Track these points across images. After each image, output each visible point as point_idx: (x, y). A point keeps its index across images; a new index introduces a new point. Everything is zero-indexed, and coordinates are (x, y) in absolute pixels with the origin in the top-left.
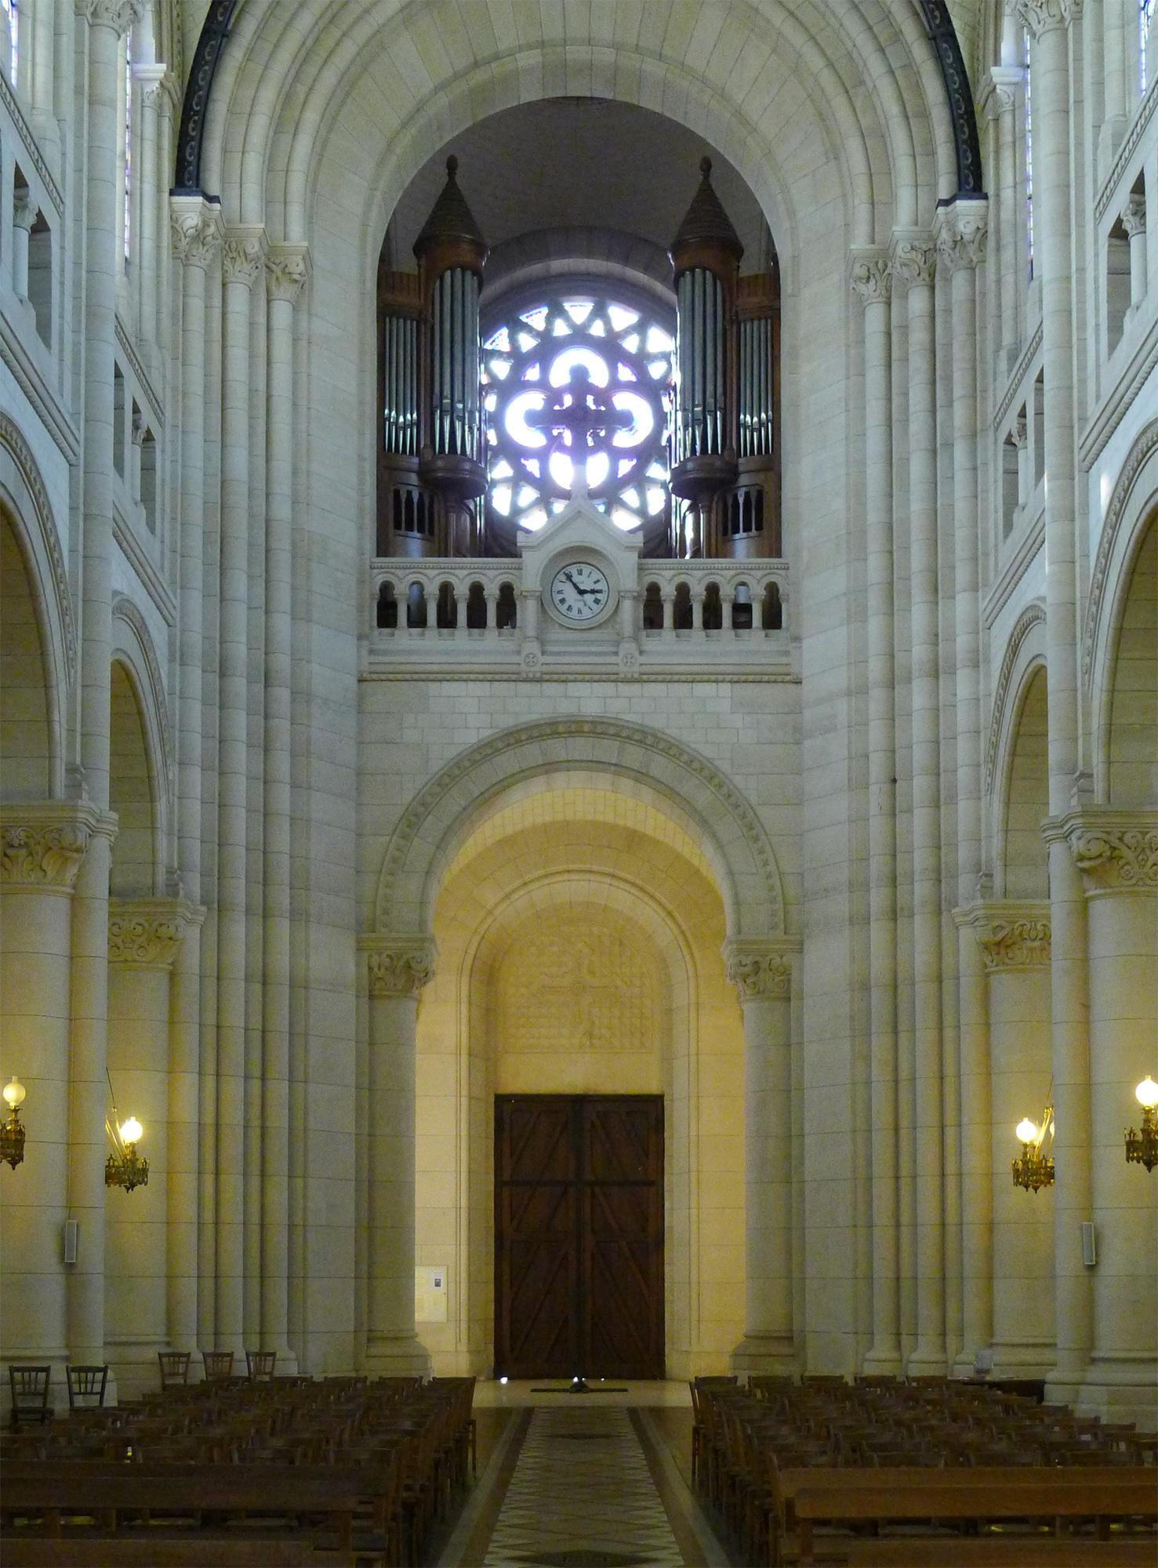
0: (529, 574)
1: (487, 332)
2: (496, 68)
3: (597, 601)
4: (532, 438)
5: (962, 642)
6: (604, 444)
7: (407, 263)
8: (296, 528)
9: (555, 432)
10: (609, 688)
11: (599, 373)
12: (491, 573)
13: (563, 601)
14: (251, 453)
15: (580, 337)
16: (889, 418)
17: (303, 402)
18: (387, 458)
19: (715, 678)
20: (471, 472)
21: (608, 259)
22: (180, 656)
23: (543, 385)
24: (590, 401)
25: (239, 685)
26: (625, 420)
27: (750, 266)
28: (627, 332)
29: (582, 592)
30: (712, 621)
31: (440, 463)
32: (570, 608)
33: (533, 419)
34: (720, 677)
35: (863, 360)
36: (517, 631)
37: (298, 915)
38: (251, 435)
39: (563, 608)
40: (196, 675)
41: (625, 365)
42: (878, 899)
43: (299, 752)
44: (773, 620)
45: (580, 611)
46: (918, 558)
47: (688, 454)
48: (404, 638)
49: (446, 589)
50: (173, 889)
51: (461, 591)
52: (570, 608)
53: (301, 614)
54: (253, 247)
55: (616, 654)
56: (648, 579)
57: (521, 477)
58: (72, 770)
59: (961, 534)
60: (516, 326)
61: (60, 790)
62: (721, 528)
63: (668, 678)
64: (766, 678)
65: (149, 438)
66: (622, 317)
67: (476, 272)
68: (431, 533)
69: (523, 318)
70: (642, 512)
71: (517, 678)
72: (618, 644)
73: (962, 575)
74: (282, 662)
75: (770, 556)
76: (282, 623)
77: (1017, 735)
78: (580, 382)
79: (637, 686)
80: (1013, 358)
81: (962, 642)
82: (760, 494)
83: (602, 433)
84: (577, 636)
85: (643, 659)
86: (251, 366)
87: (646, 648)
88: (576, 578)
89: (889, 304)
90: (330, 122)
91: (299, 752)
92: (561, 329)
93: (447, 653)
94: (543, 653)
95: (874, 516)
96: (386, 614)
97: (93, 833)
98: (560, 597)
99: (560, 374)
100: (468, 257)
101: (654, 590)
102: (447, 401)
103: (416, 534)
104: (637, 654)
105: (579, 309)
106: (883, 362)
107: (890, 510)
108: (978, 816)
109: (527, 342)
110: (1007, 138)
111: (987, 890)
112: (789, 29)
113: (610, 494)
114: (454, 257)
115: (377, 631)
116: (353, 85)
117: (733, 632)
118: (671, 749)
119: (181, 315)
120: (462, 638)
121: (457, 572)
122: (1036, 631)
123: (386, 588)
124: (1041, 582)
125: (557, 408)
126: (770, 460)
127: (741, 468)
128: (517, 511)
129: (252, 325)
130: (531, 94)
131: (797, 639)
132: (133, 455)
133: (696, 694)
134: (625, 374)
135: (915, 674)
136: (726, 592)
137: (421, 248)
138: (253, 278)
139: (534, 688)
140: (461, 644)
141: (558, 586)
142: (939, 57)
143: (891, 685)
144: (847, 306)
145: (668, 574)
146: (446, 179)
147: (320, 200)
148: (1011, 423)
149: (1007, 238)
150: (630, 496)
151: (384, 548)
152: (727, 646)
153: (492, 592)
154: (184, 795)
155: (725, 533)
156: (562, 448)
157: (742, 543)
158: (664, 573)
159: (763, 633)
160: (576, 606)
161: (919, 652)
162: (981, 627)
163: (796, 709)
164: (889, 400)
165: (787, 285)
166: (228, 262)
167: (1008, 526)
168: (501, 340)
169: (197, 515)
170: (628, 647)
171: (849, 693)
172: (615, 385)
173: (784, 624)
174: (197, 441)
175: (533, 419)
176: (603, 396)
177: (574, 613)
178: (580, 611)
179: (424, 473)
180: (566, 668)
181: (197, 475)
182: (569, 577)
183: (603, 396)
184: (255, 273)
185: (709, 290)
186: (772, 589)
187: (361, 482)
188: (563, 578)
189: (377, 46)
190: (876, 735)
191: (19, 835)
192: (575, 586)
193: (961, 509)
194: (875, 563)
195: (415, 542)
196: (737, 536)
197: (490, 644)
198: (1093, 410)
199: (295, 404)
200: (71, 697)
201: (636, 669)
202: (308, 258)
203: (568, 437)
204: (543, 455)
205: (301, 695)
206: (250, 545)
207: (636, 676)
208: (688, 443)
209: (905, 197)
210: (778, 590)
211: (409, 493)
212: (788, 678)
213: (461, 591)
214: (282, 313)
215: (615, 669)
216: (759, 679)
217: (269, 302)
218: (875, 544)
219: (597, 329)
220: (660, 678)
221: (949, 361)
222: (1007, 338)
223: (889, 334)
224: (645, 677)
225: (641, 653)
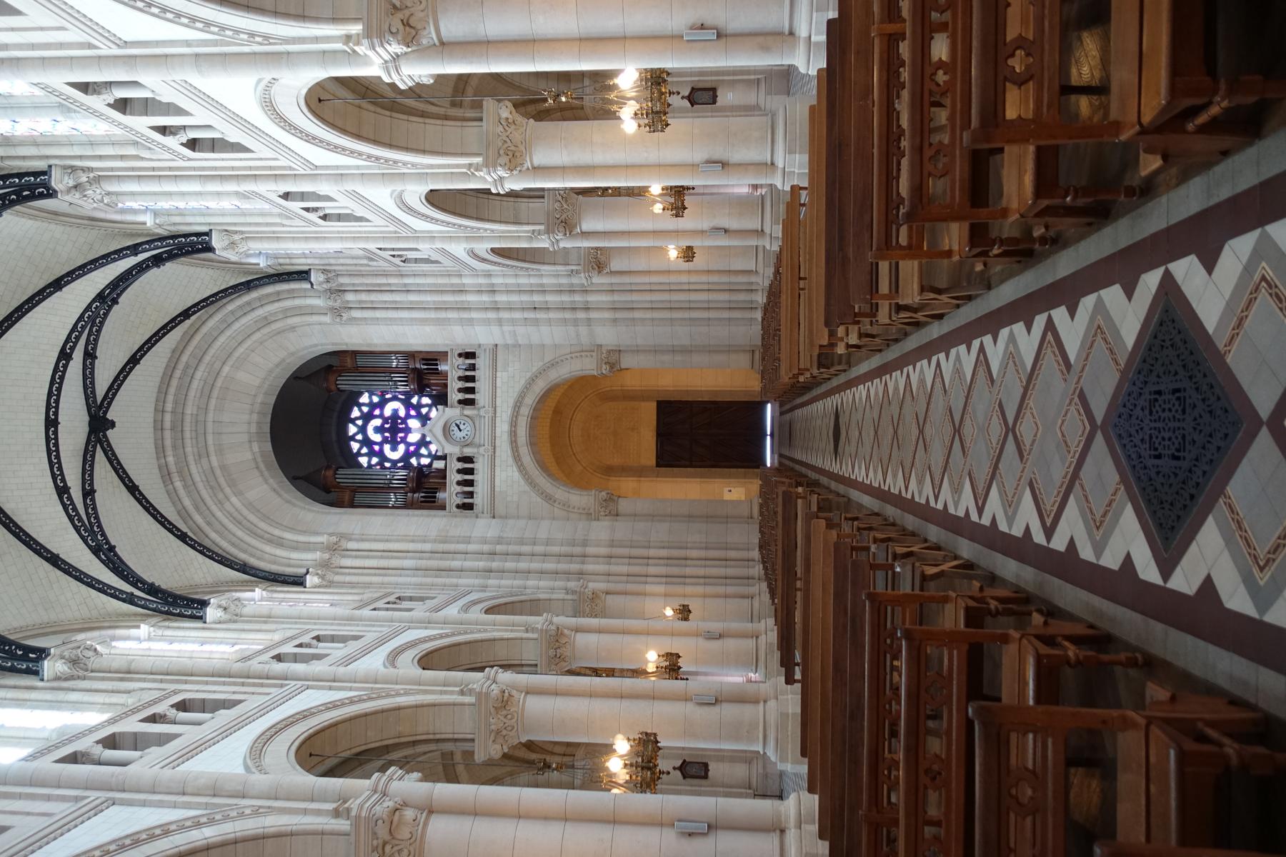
0: (453, 450)
4: (402, 448)
5: (482, 281)
6: (404, 421)
7: (333, 496)
8: (435, 541)
15: (363, 430)
18: (408, 505)
22: (484, 588)
23: (381, 444)
25: (495, 565)
27: (334, 362)
28: (361, 410)
30: (472, 379)
33: (394, 449)
37: (585, 543)
40: (491, 582)
42: (581, 315)
43: (521, 542)
44: (471, 355)
46: (449, 298)
48: (478, 500)
49: (459, 483)
50: (574, 592)
51: (460, 477)
53: (468, 540)
54: (327, 556)
58: (527, 631)
59: (440, 281)
61: (535, 636)
65: (399, 598)
70: (430, 406)
73: (455, 281)
74: (486, 548)
76: (471, 547)
77: (518, 260)
80: (372, 260)
81: (482, 281)
90: (278, 525)
91: (521, 542)
92: (359, 437)
95: (432, 315)
96: (469, 507)
97: (551, 623)
99: (377, 438)
101: (460, 402)
108: (549, 275)
110: (288, 261)
111: (578, 272)
112: (246, 345)
119: (352, 585)
122: (477, 252)
123: (458, 507)
124: (459, 249)
126: (410, 355)
129: (356, 557)
130: (269, 446)
132: (406, 604)
136: (461, 373)
139: (498, 450)
140: (480, 477)
142: (256, 287)
147: (306, 529)
148: (397, 261)
149: (326, 261)
151: (443, 508)
152: (482, 374)
153: (460, 465)
154: (537, 587)
156: (406, 437)
157: (442, 367)
162: (475, 273)
163: (506, 346)
165: (344, 348)
167: (437, 262)
168: (363, 461)
169: (429, 580)
170: (482, 412)
172: (381, 416)
174: (401, 580)
175: (394, 449)
176: (386, 420)
181: (414, 580)
183: (386, 420)
186: (460, 355)
190: (517, 315)
191: (552, 653)
194: (451, 315)
195: (440, 495)
197: (480, 466)
198: (392, 228)
200: (498, 630)
205: (499, 541)
209: (309, 301)
213: (460, 477)
216: (495, 361)
218: (443, 315)
222: (365, 262)
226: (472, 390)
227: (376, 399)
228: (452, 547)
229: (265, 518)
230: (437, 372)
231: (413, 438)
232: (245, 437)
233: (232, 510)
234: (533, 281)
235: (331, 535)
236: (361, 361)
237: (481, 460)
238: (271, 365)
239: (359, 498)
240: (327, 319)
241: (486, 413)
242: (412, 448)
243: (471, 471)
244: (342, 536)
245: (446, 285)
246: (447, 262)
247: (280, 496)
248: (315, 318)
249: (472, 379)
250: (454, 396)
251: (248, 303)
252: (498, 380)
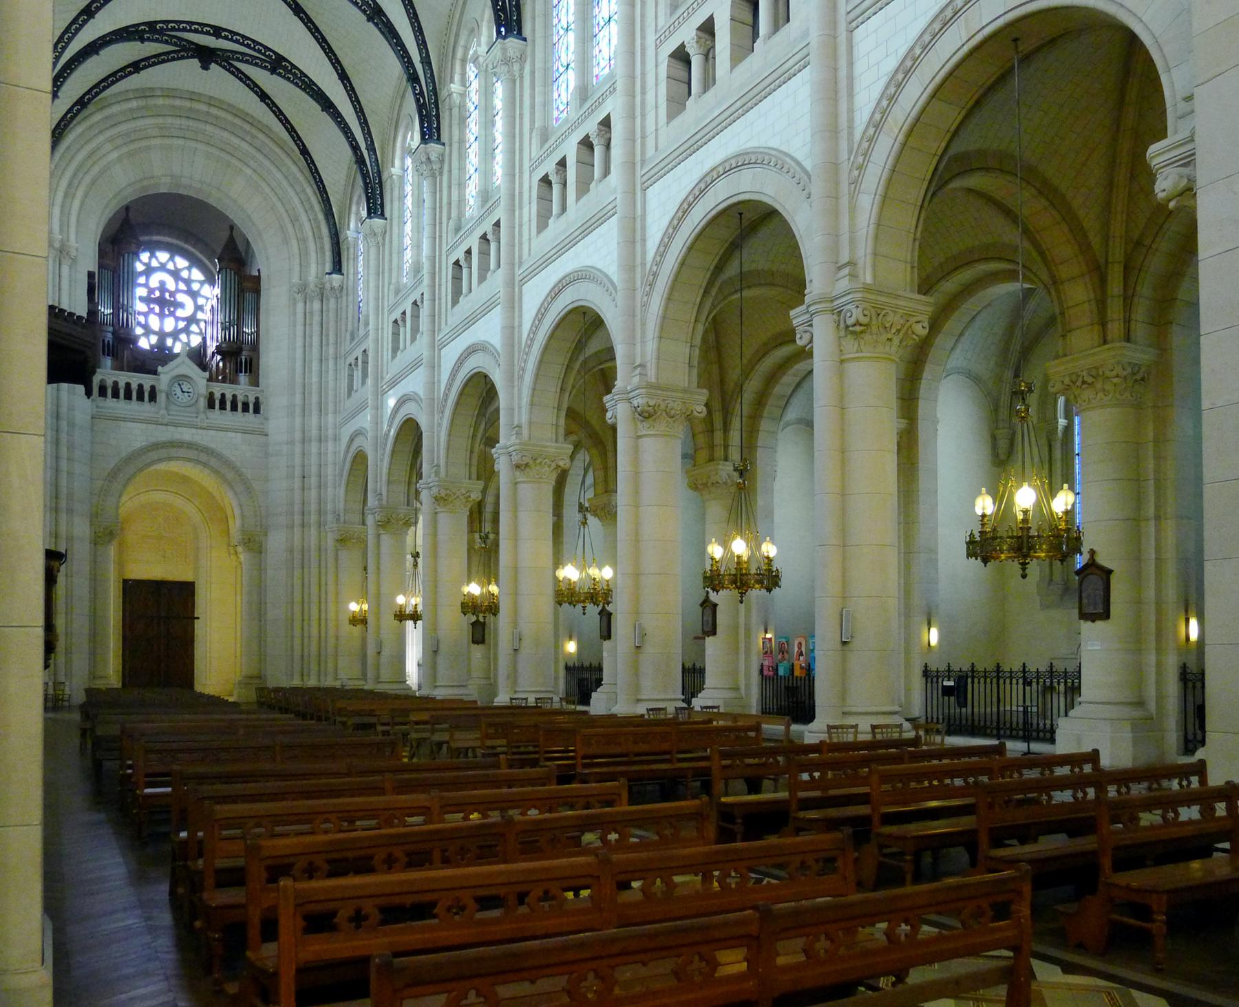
5: (330, 432)
6: (172, 314)
10: (194, 431)
11: (171, 284)
15: (163, 267)
19: (235, 431)
24: (167, 295)
44: (257, 410)
46: (315, 398)
59: (331, 393)
63: (218, 429)
66: (181, 263)
73: (331, 407)
78: (162, 287)
81: (330, 432)
92: (154, 263)
95: (299, 380)
101: (211, 394)
105: (163, 256)
108: (336, 495)
111: (338, 520)
118: (219, 456)
120: (134, 405)
124: (365, 420)
126: (255, 347)
131: (267, 419)
133: (226, 435)
134: (182, 286)
139: (164, 428)
143: (303, 442)
150: (183, 337)
153: (147, 388)
157: (243, 378)
161: (314, 432)
170: (202, 416)
172: (178, 291)
183: (172, 294)
186: (257, 398)
190: (298, 461)
193: (331, 384)
194: (298, 399)
203: (157, 309)
204: (146, 315)
216: (252, 433)
218: (299, 390)
219: (170, 266)
221: (328, 328)
222: (350, 327)
226: (223, 407)
234: (330, 478)
243: (140, 398)
245: (327, 398)
246: (350, 404)
250: (218, 389)
252: (233, 435)
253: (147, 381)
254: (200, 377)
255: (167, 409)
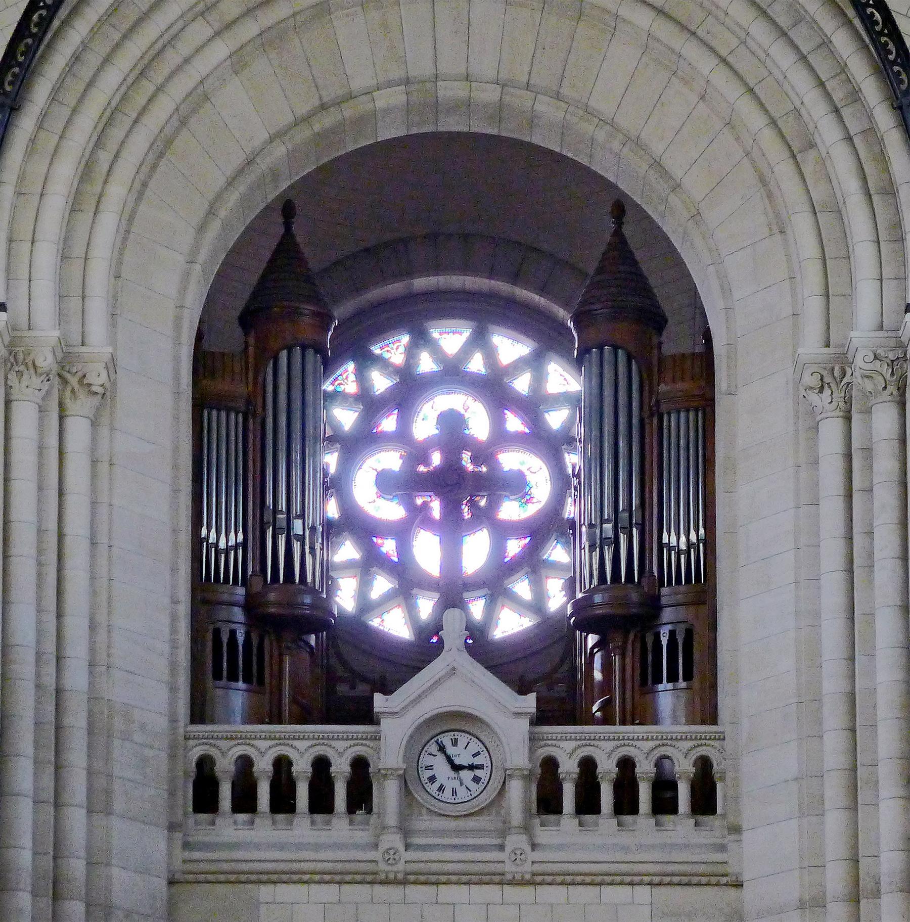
1: (329, 365)
2: (348, 111)
3: (477, 780)
7: (230, 338)
9: (419, 501)
10: (492, 892)
11: (479, 424)
12: (340, 745)
13: (432, 779)
14: (39, 610)
15: (452, 374)
16: (851, 561)
17: (103, 539)
19: (631, 880)
20: (312, 606)
21: (490, 277)
26: (517, 486)
27: (676, 341)
29: (457, 768)
31: (272, 596)
32: (441, 788)
33: (386, 484)
34: (637, 879)
35: (815, 484)
36: (373, 819)
38: (40, 585)
39: (433, 788)
41: (516, 414)
44: (705, 801)
45: (454, 792)
47: (595, 581)
52: (441, 788)
55: (501, 847)
56: (542, 753)
57: (372, 561)
60: (365, 360)
62: (637, 677)
64: (695, 880)
66: (510, 347)
67: (320, 349)
68: (261, 682)
69: (376, 350)
71: (372, 879)
72: (503, 833)
75: (703, 722)
79: (529, 889)
82: (689, 634)
83: (483, 503)
84: (452, 824)
85: (537, 855)
86: (40, 500)
87: (538, 840)
88: (450, 750)
89: (848, 419)
92: (426, 364)
93: (282, 847)
94: (407, 847)
95: (832, 684)
98: (429, 773)
99: (425, 427)
100: (307, 333)
101: (550, 765)
102: (282, 517)
103: (241, 684)
104: (528, 849)
105: (451, 338)
106: (841, 492)
107: (852, 677)
109: (380, 382)
113: (495, 583)
114: (287, 303)
115: (191, 821)
116: (169, 142)
117: (652, 821)
120: (302, 827)
121: (296, 743)
125: (422, 469)
126: (702, 590)
127: (664, 601)
128: (366, 606)
130: (390, 131)
134: (514, 423)
135: (884, 888)
136: (645, 769)
137: (248, 320)
138: (43, 392)
139: (394, 892)
141: (426, 760)
143: (855, 898)
144: (797, 417)
145: (569, 745)
146: (281, 230)
150: (522, 588)
151: (200, 712)
152: (647, 838)
153: (341, 768)
155: (644, 682)
156: (428, 523)
157: (667, 698)
158: (563, 744)
159: (692, 821)
160: (449, 785)
164: (850, 539)
166: (12, 376)
168: (346, 380)
171: (802, 906)
172: (501, 438)
173: (719, 810)
175: (386, 484)
176: (484, 454)
177: (447, 795)
178: (454, 792)
179: (251, 606)
180: (435, 867)
182: (442, 749)
183: (484, 454)
184: (46, 387)
185: (622, 369)
187: (174, 631)
188: (433, 748)
189: (200, 97)
192: (449, 760)
196: (661, 687)
199: (93, 544)
201: (528, 868)
202: (112, 365)
203: (436, 508)
206: (38, 724)
207: (528, 877)
208: (595, 566)
210: (711, 766)
211: (233, 633)
212: (724, 880)
214: (78, 430)
215: (499, 868)
216: (688, 881)
217: (62, 418)
218: (833, 717)
219: (477, 364)
220: (559, 879)
223: (848, 457)
224: (539, 879)
225: (534, 846)
226: (588, 804)
227: (556, 419)
228: (77, 756)
229: (162, 147)
230: (648, 678)
231: (427, 552)
232: (421, 67)
233: (184, 48)
235: (112, 365)
236: (679, 426)
237: (362, 836)
238: (658, 148)
239: (225, 425)
240: (811, 346)
241: (516, 853)
242: (389, 546)
243: (321, 803)
244: (106, 397)
247: (231, 183)
248: (813, 306)
249: (626, 804)
250: (567, 746)
251: (855, 95)
252: (623, 893)
253: (340, 744)
254: (507, 713)
255: (405, 831)
